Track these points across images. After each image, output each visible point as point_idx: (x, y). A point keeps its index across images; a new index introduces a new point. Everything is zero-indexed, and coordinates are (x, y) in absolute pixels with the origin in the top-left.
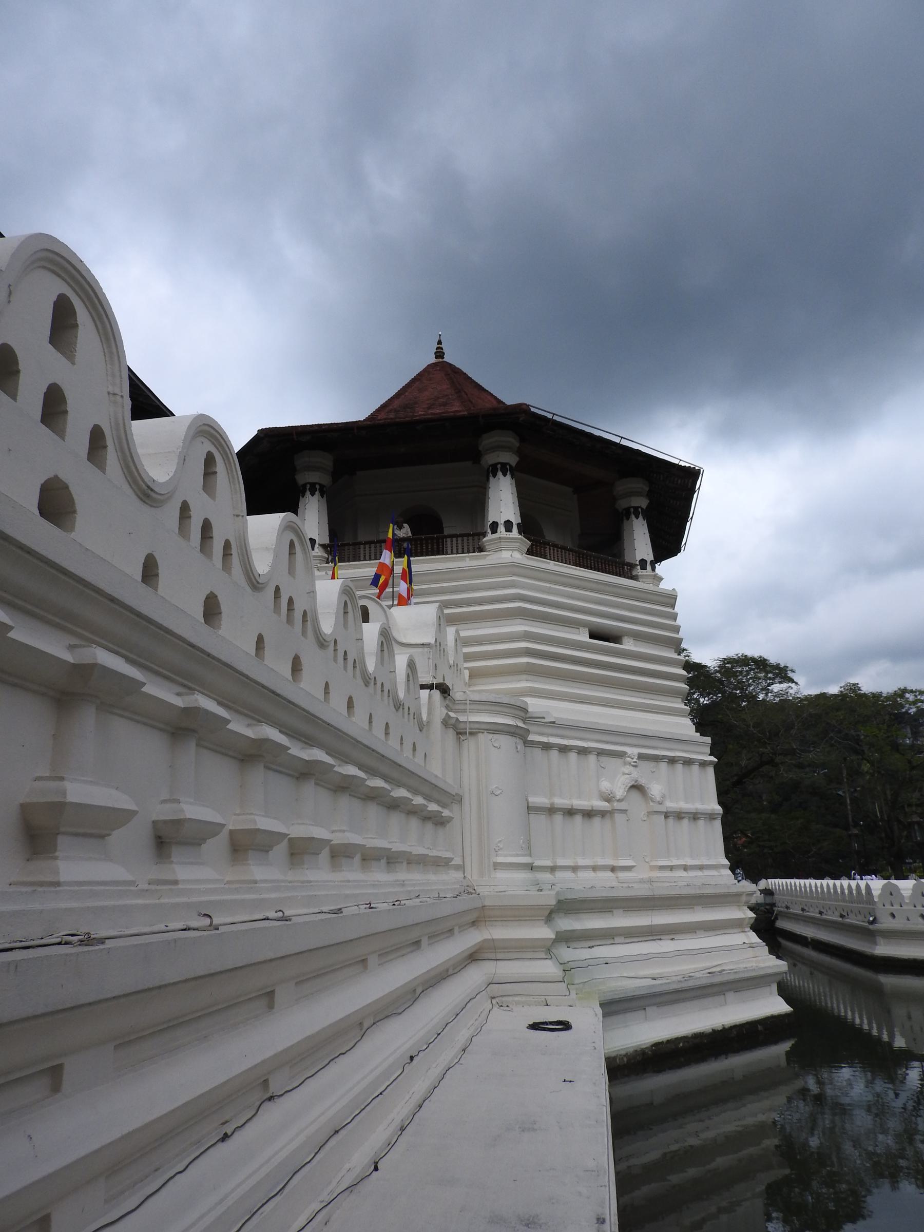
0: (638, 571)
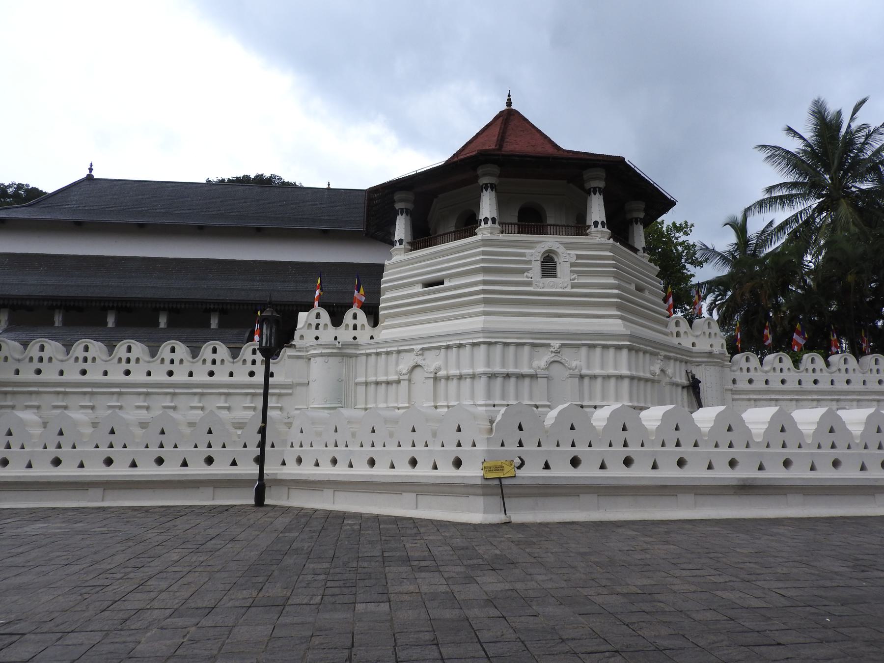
0: (593, 229)
